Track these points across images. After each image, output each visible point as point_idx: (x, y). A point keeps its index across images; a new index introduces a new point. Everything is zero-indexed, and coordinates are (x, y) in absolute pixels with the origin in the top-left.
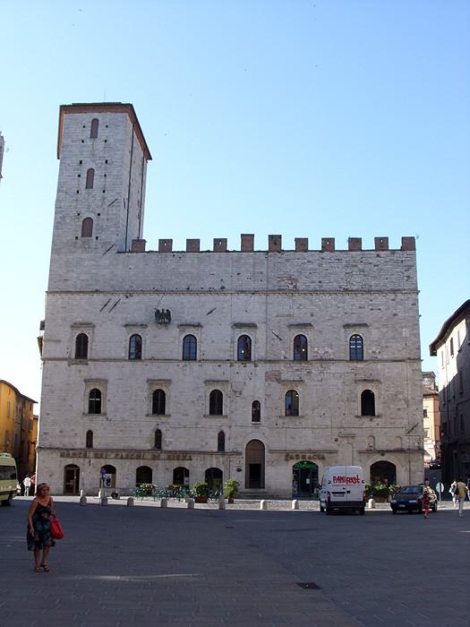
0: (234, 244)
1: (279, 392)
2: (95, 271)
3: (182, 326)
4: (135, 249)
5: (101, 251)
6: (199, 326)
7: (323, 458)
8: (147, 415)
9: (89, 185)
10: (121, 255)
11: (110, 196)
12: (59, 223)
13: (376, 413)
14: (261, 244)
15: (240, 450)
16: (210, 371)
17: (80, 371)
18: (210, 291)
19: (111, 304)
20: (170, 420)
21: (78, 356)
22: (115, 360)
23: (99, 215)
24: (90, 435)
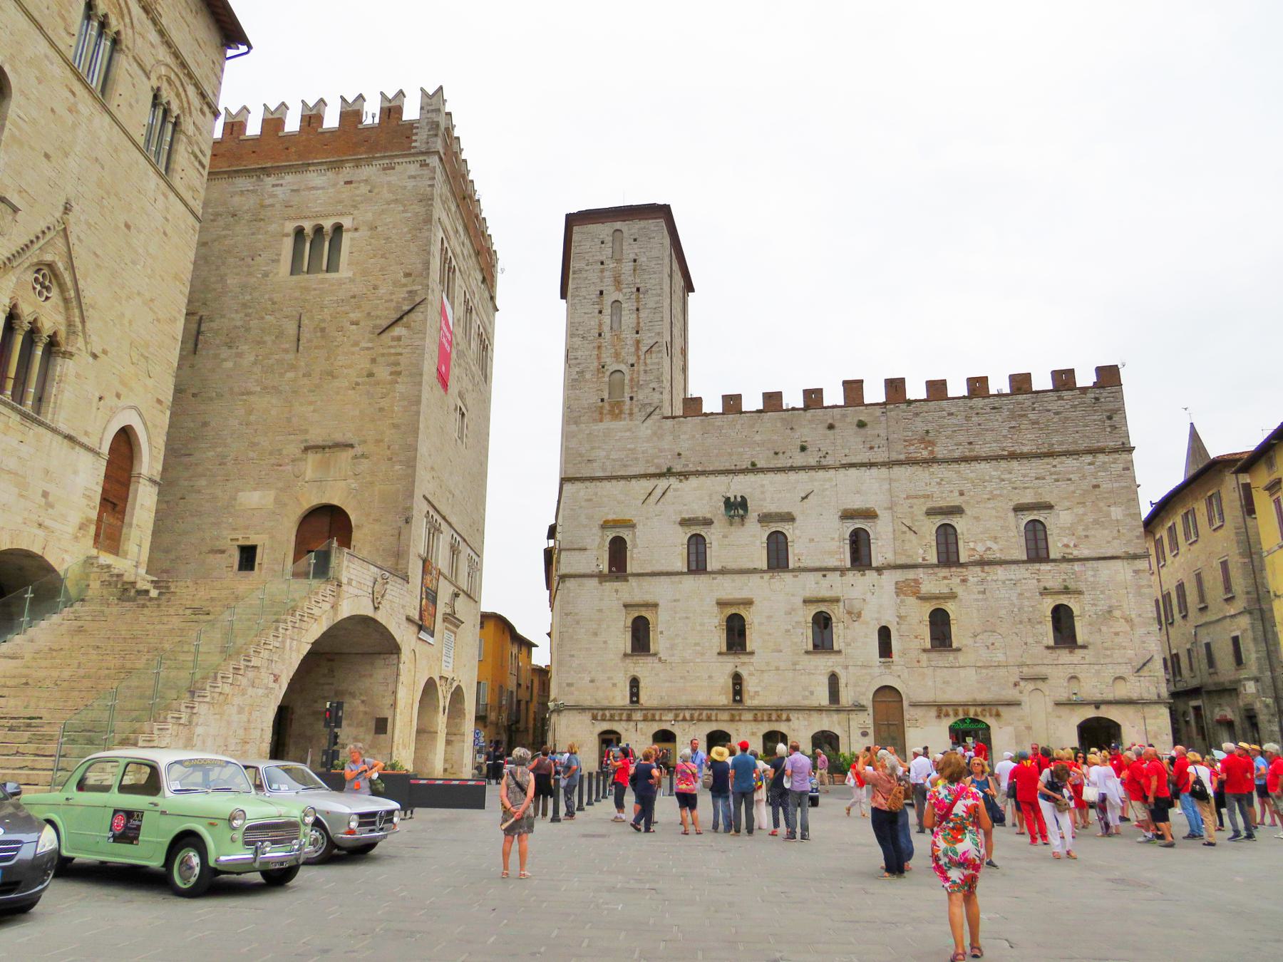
3: (765, 519)
5: (639, 416)
6: (789, 518)
8: (720, 654)
10: (669, 422)
12: (575, 380)
13: (1081, 638)
14: (874, 393)
15: (864, 703)
16: (812, 585)
17: (617, 591)
19: (658, 492)
20: (754, 659)
24: (635, 683)
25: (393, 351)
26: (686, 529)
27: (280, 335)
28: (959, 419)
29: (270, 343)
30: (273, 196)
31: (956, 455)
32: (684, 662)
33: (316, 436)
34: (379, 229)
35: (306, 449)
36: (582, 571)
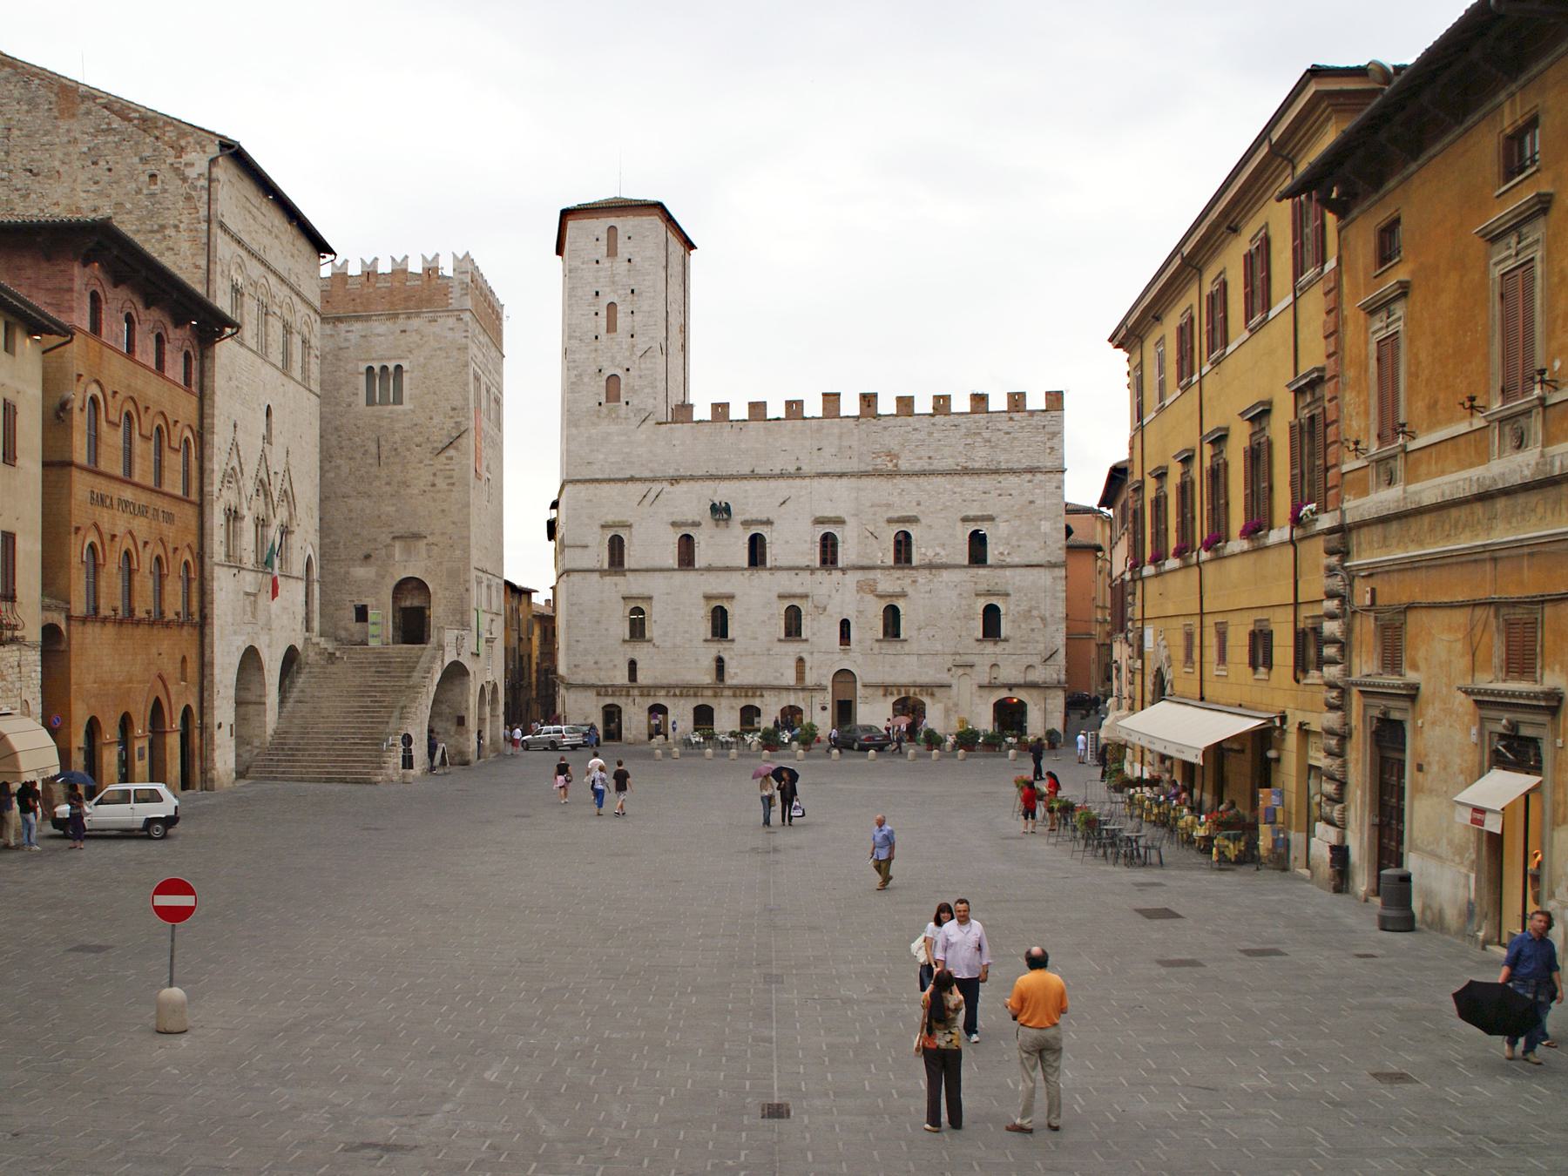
0: (813, 408)
1: (876, 609)
3: (746, 524)
5: (635, 421)
6: (769, 522)
7: (932, 695)
9: (611, 327)
11: (642, 343)
13: (1003, 634)
14: (850, 406)
18: (781, 476)
19: (652, 494)
20: (734, 646)
21: (612, 564)
22: (661, 570)
24: (633, 665)
28: (922, 435)
30: (346, 340)
31: (917, 468)
32: (675, 646)
33: (399, 528)
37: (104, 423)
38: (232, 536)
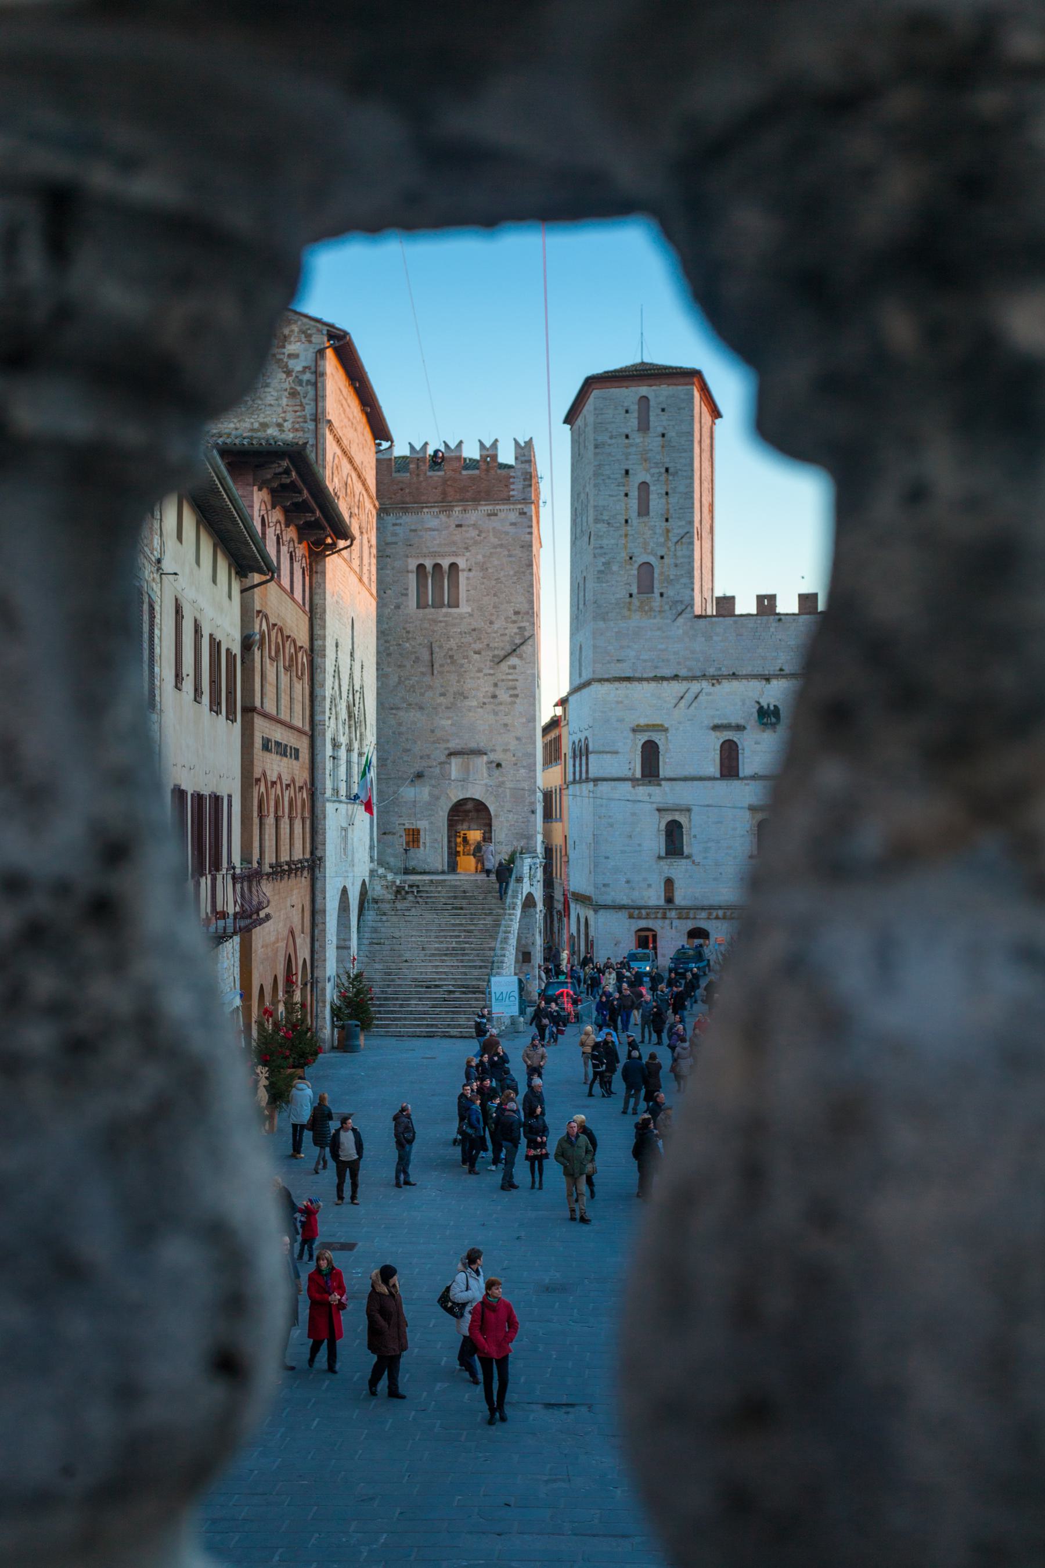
2: (660, 647)
4: (723, 612)
9: (644, 510)
10: (702, 621)
17: (650, 795)
19: (689, 696)
23: (662, 557)
24: (669, 883)
25: (510, 677)
26: (718, 734)
27: (417, 660)
29: (408, 667)
30: (395, 534)
33: (454, 744)
34: (490, 570)
35: (450, 754)
36: (615, 775)
37: (268, 660)
38: (336, 767)
